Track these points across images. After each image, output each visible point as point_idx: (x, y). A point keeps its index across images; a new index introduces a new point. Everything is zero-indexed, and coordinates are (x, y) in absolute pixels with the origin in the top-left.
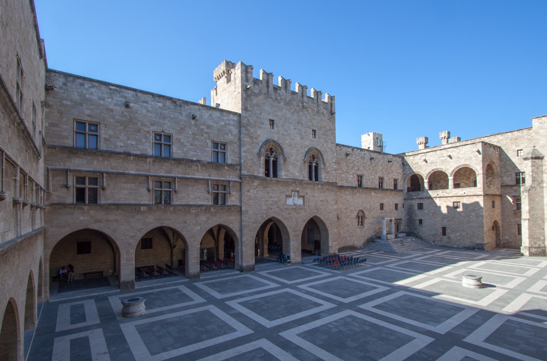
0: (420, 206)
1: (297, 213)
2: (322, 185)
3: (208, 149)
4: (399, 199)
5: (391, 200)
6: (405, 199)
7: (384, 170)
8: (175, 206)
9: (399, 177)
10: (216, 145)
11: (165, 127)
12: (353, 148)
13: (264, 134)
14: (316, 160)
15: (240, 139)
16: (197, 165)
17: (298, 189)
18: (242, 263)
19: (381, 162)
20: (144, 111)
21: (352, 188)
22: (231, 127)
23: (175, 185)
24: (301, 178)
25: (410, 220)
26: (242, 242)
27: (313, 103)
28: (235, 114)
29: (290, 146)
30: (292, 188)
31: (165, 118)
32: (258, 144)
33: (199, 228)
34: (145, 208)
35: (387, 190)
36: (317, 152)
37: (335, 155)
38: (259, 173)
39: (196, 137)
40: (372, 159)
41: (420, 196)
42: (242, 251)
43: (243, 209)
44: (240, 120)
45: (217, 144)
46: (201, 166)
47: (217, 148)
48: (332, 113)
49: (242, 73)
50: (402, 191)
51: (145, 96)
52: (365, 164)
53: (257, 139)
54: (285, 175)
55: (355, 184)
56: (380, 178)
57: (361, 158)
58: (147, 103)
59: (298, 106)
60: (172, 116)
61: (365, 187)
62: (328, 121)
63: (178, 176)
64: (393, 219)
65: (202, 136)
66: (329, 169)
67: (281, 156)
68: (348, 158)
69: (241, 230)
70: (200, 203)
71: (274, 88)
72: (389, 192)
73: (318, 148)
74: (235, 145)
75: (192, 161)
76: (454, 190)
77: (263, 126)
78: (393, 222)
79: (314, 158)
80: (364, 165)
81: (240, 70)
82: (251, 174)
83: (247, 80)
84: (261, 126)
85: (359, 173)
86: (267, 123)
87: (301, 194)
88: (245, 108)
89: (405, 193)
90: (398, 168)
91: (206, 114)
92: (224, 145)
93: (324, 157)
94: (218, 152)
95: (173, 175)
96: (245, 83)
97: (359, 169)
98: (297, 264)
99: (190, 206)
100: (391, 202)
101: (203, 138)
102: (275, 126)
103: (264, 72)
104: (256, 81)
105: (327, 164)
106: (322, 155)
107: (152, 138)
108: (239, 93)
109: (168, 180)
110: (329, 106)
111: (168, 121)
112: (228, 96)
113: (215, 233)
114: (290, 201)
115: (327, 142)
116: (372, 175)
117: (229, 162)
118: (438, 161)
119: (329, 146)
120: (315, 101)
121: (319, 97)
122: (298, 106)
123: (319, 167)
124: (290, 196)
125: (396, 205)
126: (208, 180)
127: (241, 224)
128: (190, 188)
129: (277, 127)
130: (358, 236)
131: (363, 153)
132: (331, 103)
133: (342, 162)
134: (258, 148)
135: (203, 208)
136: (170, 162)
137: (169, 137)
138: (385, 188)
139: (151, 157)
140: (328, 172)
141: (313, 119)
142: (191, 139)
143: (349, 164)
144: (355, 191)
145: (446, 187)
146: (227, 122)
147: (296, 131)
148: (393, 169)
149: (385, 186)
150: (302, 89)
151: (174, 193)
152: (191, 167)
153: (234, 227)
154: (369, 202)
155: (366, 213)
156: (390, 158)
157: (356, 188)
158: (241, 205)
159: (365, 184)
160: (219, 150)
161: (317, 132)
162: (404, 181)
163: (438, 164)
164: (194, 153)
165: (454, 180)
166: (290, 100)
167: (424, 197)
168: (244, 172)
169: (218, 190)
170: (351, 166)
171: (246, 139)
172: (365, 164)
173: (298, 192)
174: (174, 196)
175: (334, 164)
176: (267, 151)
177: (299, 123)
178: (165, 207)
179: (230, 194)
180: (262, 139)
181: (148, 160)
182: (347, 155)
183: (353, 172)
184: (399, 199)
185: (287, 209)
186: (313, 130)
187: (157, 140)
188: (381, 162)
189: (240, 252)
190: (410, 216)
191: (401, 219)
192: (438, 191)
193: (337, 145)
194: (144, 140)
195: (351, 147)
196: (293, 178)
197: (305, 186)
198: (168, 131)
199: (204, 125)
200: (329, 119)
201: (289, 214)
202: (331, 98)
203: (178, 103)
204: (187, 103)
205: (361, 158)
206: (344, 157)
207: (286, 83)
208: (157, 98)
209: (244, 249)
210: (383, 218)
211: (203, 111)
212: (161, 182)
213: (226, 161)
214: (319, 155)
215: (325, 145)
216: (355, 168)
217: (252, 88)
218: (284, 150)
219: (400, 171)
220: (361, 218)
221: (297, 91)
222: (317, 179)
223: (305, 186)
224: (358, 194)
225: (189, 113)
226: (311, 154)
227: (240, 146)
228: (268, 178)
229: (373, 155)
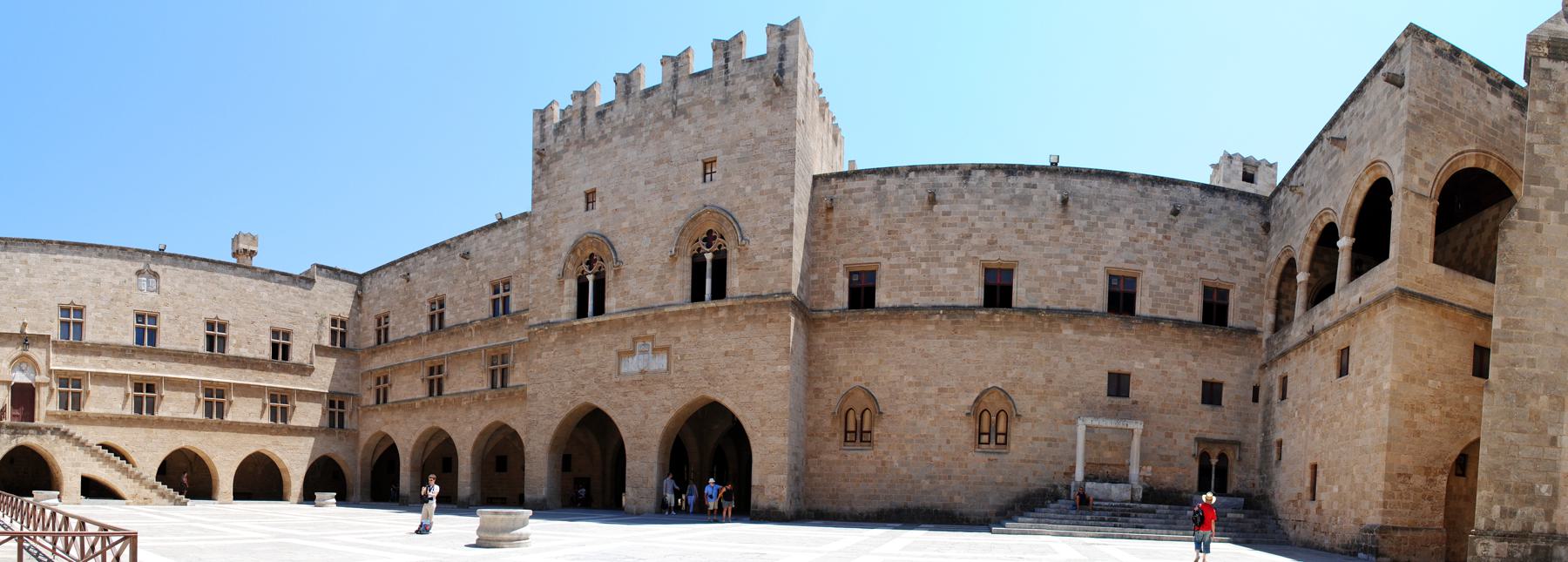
1: (648, 393)
17: (650, 332)
21: (953, 311)
30: (635, 332)
59: (660, 118)
61: (1026, 304)
87: (660, 343)
97: (992, 243)
114: (632, 365)
122: (660, 118)
124: (632, 353)
133: (907, 226)
143: (942, 231)
144: (968, 321)
147: (652, 186)
155: (1023, 402)
166: (639, 116)
173: (652, 338)
177: (659, 162)
182: (933, 201)
183: (960, 254)
185: (619, 384)
197: (671, 320)
201: (625, 394)
216: (975, 241)
223: (671, 320)
224: (980, 333)
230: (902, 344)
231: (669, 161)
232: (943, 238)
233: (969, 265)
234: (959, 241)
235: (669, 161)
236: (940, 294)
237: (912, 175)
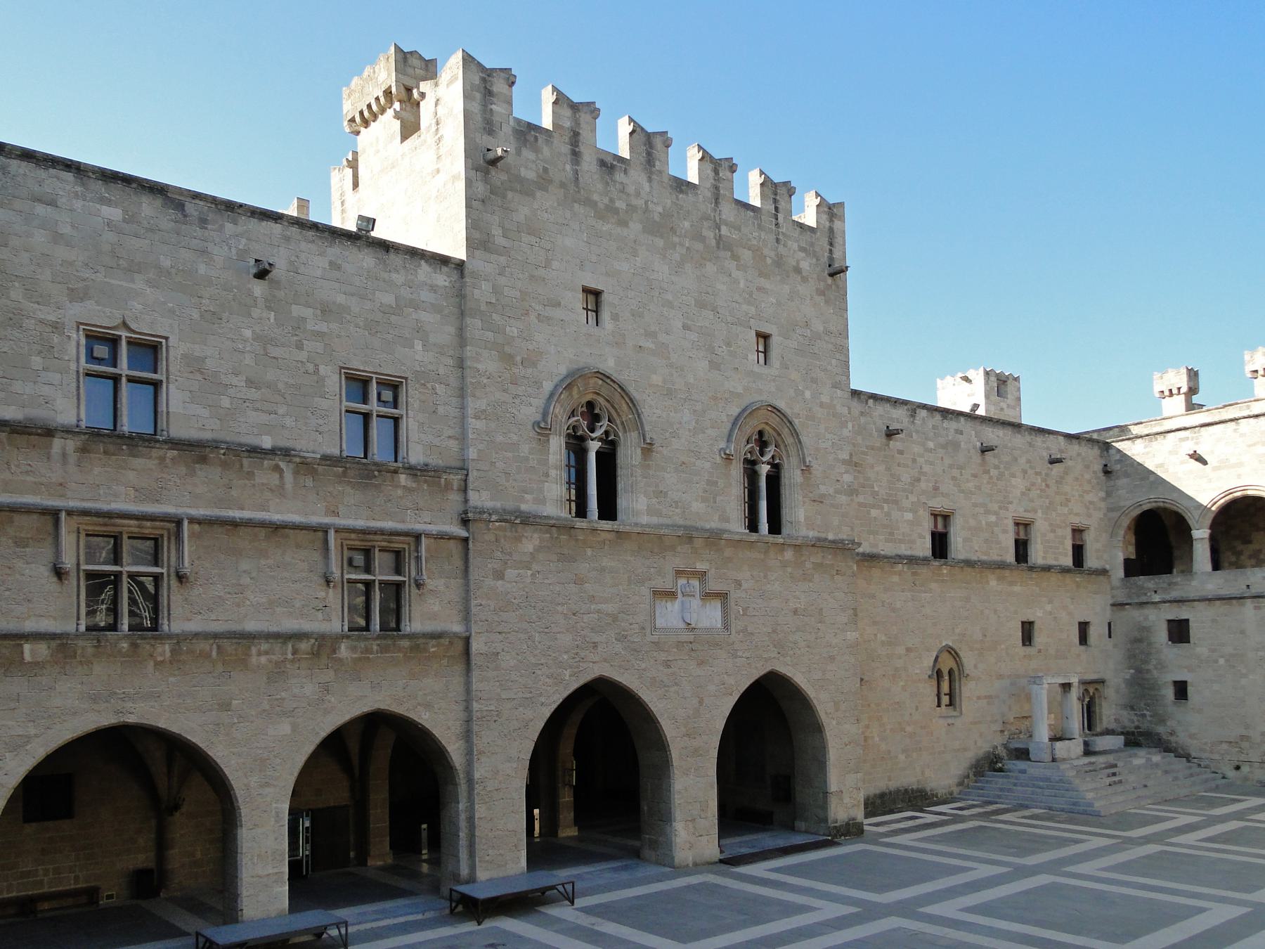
2: (797, 547)
3: (325, 404)
4: (1092, 604)
5: (1060, 608)
7: (1035, 493)
8: (180, 638)
9: (1093, 521)
10: (359, 384)
11: (137, 306)
12: (914, 408)
13: (565, 344)
14: (770, 451)
15: (461, 364)
16: (277, 468)
18: (473, 868)
19: (1022, 461)
20: (40, 238)
21: (912, 560)
22: (425, 316)
23: (180, 550)
24: (714, 524)
25: (1141, 687)
26: (470, 781)
27: (760, 227)
28: (442, 261)
29: (670, 393)
31: (133, 269)
32: (538, 384)
33: (285, 728)
34: (42, 650)
35: (1047, 569)
36: (774, 420)
37: (846, 432)
38: (542, 501)
39: (275, 352)
40: (985, 450)
41: (1175, 594)
42: (471, 820)
43: (475, 646)
44: (463, 286)
45: (365, 382)
46: (296, 473)
47: (365, 400)
48: (837, 272)
49: (467, 96)
50: (1103, 572)
51: (41, 173)
52: (961, 468)
53: (534, 365)
54: (650, 511)
55: (924, 547)
56: (1017, 524)
57: (944, 447)
58: (52, 203)
59: (701, 238)
60: (166, 263)
62: (820, 300)
63: (193, 512)
64: (1074, 680)
65: (300, 346)
66: (823, 489)
67: (634, 435)
68: (895, 444)
69: (467, 735)
70: (290, 624)
71: (602, 163)
72: (1054, 578)
73: (781, 405)
74: (440, 389)
75: (255, 451)
77: (557, 313)
78: (1075, 693)
79: (763, 444)
80: (955, 472)
81: (458, 86)
82: (510, 505)
83: (489, 127)
84: (549, 312)
85: (939, 504)
86: (577, 301)
88: (477, 238)
90: (1088, 487)
91: (317, 259)
92: (395, 387)
93: (803, 439)
94: (366, 417)
95: (170, 509)
96: (486, 141)
97: (936, 489)
98: (700, 866)
99: (249, 638)
101: (303, 356)
102: (605, 315)
103: (561, 100)
104: (528, 132)
105: (817, 469)
106: (795, 433)
107: (73, 347)
108: (455, 178)
109: (149, 528)
110: (824, 242)
111: (149, 282)
112: (414, 192)
113: (354, 746)
115: (814, 381)
116: (987, 512)
117: (416, 455)
119: (825, 399)
120: (768, 222)
121: (782, 205)
123: (785, 481)
125: (1084, 628)
126: (324, 530)
127: (468, 709)
128: (245, 565)
129: (615, 317)
130: (940, 752)
131: (952, 425)
132: (831, 230)
134: (539, 402)
135: (304, 646)
136: (155, 453)
137: (150, 350)
139: (68, 431)
140: (819, 501)
141: (759, 289)
142: (249, 359)
144: (924, 571)
146: (405, 293)
147: (693, 336)
148: (1067, 488)
149: (1037, 554)
150: (716, 172)
151: (174, 582)
152: (250, 475)
153: (442, 724)
154: (976, 614)
156: (1056, 447)
157: (925, 559)
158: (468, 629)
159: (959, 546)
160: (373, 406)
161: (775, 341)
164: (264, 418)
167: (1192, 595)
168: (480, 498)
169: (368, 569)
170: (906, 478)
171: (486, 363)
172: (961, 468)
173: (702, 575)
174: (177, 598)
175: (843, 469)
176: (573, 414)
177: (701, 305)
178: (134, 646)
179: (419, 585)
180: (555, 366)
181: (57, 444)
182: (890, 434)
183: (913, 498)
184: (1092, 604)
186: (760, 335)
187: (100, 361)
188: (1022, 461)
189: (463, 824)
190: (1139, 671)
193: (855, 393)
194: (37, 362)
195: (905, 403)
196: (681, 522)
197: (728, 552)
198: (145, 327)
199: (308, 305)
200: (821, 293)
202: (831, 211)
203: (190, 208)
204: (230, 208)
205: (944, 447)
206: (879, 440)
207: (650, 144)
208: (98, 186)
209: (480, 811)
210: (1036, 680)
211: (303, 245)
212: (117, 538)
213: (402, 453)
214: (785, 432)
215: (808, 394)
216: (923, 485)
217: (510, 159)
218: (646, 412)
219: (1095, 496)
220: (948, 680)
221: (693, 176)
222: (775, 527)
225: (243, 254)
226: (751, 428)
227: (462, 393)
228: (580, 523)
229: (993, 435)
230: (873, 597)
231: (714, 310)
232: (899, 480)
233: (921, 512)
234: (912, 484)
235: (714, 310)
236: (901, 541)
237: (871, 401)
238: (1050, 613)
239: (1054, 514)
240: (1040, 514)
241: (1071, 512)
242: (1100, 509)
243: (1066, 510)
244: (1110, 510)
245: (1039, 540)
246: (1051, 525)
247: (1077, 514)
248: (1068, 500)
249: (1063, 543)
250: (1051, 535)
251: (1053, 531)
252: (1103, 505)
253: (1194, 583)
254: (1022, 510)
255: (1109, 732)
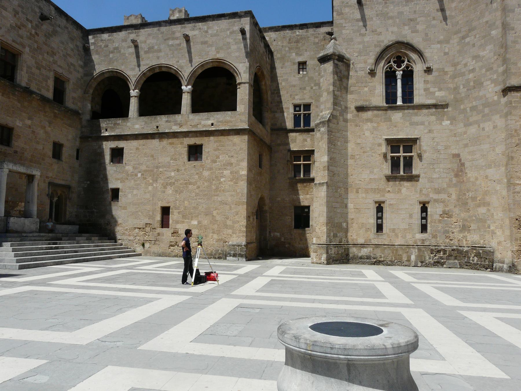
0: (118, 155)
6: (84, 138)
50: (76, 113)
76: (192, 116)
89: (84, 123)
100: (41, 132)
118: (162, 47)
138: (24, 84)
145: (176, 109)
162: (85, 92)
163: (161, 54)
165: (194, 94)
184: (67, 135)
191: (68, 187)
192: (158, 117)
238: (30, 127)
239: (40, 57)
240: (27, 49)
241: (55, 62)
242: (78, 72)
243: (51, 59)
244: (86, 75)
245: (25, 69)
246: (36, 63)
247: (59, 66)
248: (53, 54)
249: (47, 81)
250: (37, 72)
251: (38, 68)
252: (81, 70)
253: (129, 124)
254: (10, 39)
255: (69, 223)
